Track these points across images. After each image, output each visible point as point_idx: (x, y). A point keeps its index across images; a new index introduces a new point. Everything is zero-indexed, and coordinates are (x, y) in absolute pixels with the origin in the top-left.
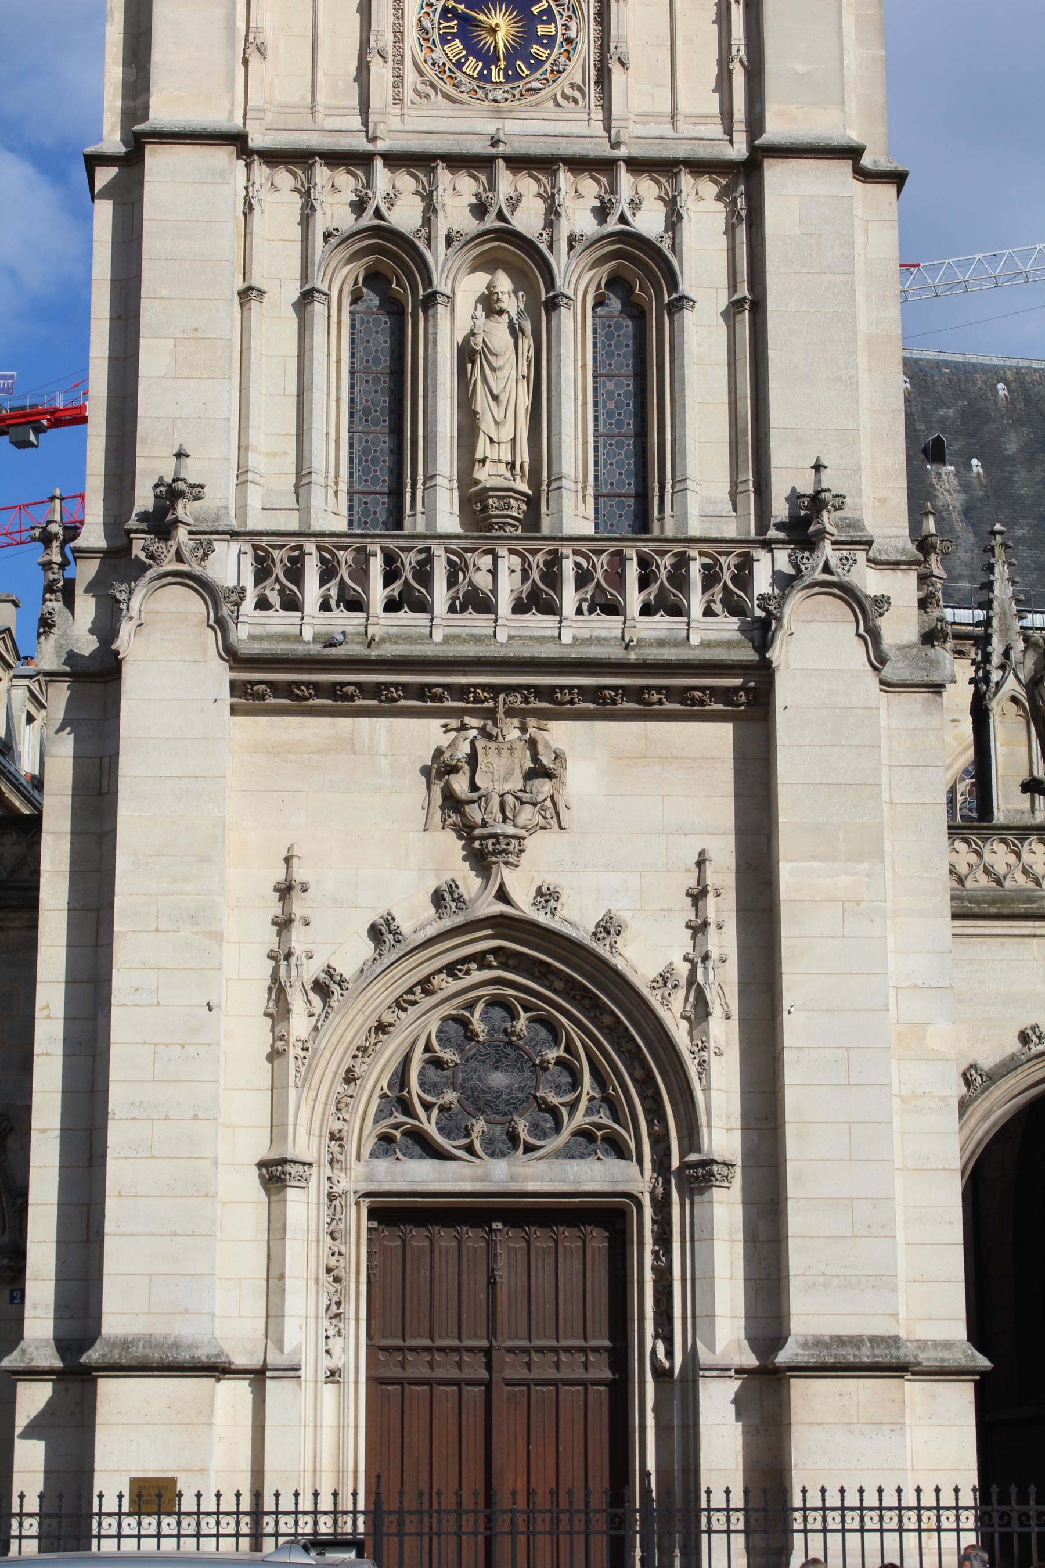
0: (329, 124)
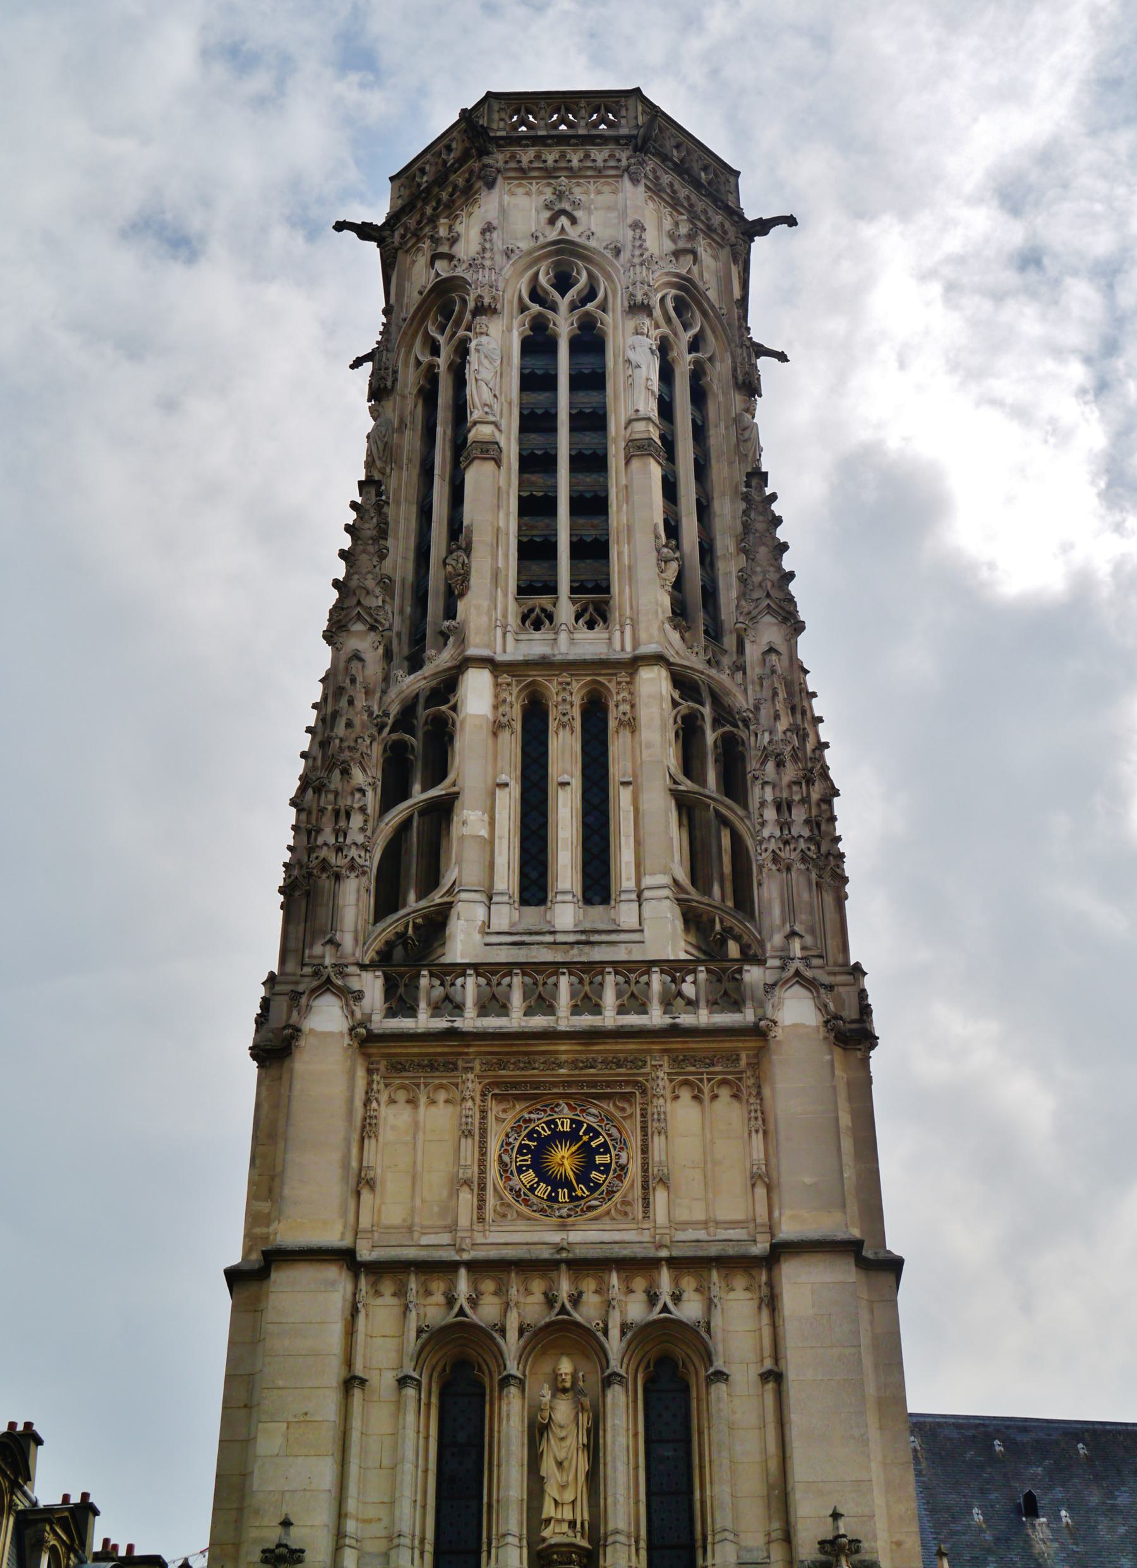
0: (424, 1241)
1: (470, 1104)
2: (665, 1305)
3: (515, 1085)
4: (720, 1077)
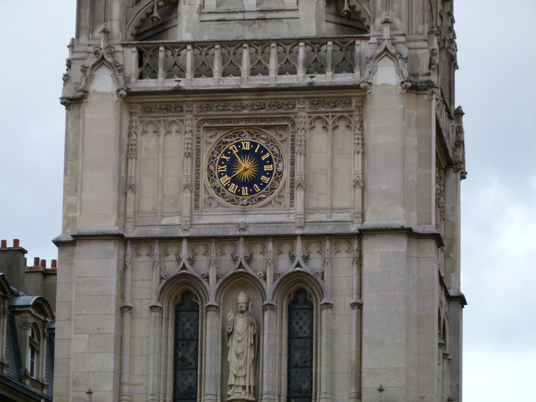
0: (165, 221)
1: (189, 136)
2: (298, 263)
3: (216, 121)
4: (339, 114)
